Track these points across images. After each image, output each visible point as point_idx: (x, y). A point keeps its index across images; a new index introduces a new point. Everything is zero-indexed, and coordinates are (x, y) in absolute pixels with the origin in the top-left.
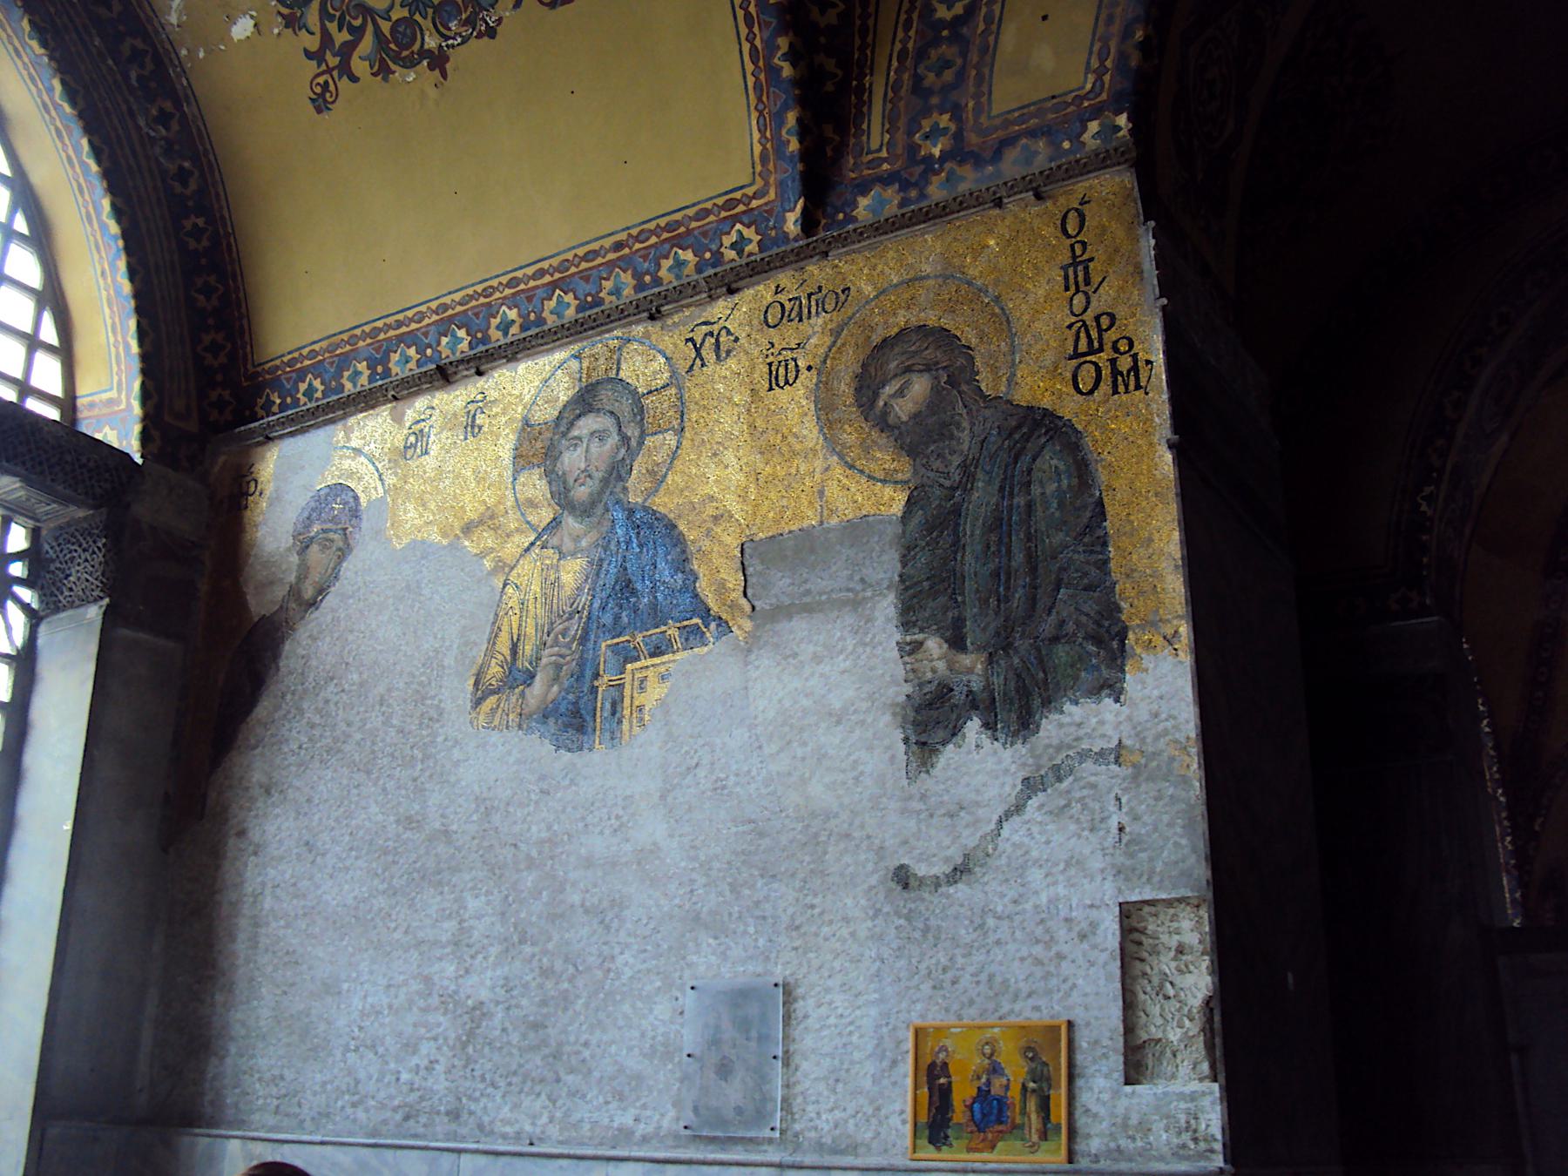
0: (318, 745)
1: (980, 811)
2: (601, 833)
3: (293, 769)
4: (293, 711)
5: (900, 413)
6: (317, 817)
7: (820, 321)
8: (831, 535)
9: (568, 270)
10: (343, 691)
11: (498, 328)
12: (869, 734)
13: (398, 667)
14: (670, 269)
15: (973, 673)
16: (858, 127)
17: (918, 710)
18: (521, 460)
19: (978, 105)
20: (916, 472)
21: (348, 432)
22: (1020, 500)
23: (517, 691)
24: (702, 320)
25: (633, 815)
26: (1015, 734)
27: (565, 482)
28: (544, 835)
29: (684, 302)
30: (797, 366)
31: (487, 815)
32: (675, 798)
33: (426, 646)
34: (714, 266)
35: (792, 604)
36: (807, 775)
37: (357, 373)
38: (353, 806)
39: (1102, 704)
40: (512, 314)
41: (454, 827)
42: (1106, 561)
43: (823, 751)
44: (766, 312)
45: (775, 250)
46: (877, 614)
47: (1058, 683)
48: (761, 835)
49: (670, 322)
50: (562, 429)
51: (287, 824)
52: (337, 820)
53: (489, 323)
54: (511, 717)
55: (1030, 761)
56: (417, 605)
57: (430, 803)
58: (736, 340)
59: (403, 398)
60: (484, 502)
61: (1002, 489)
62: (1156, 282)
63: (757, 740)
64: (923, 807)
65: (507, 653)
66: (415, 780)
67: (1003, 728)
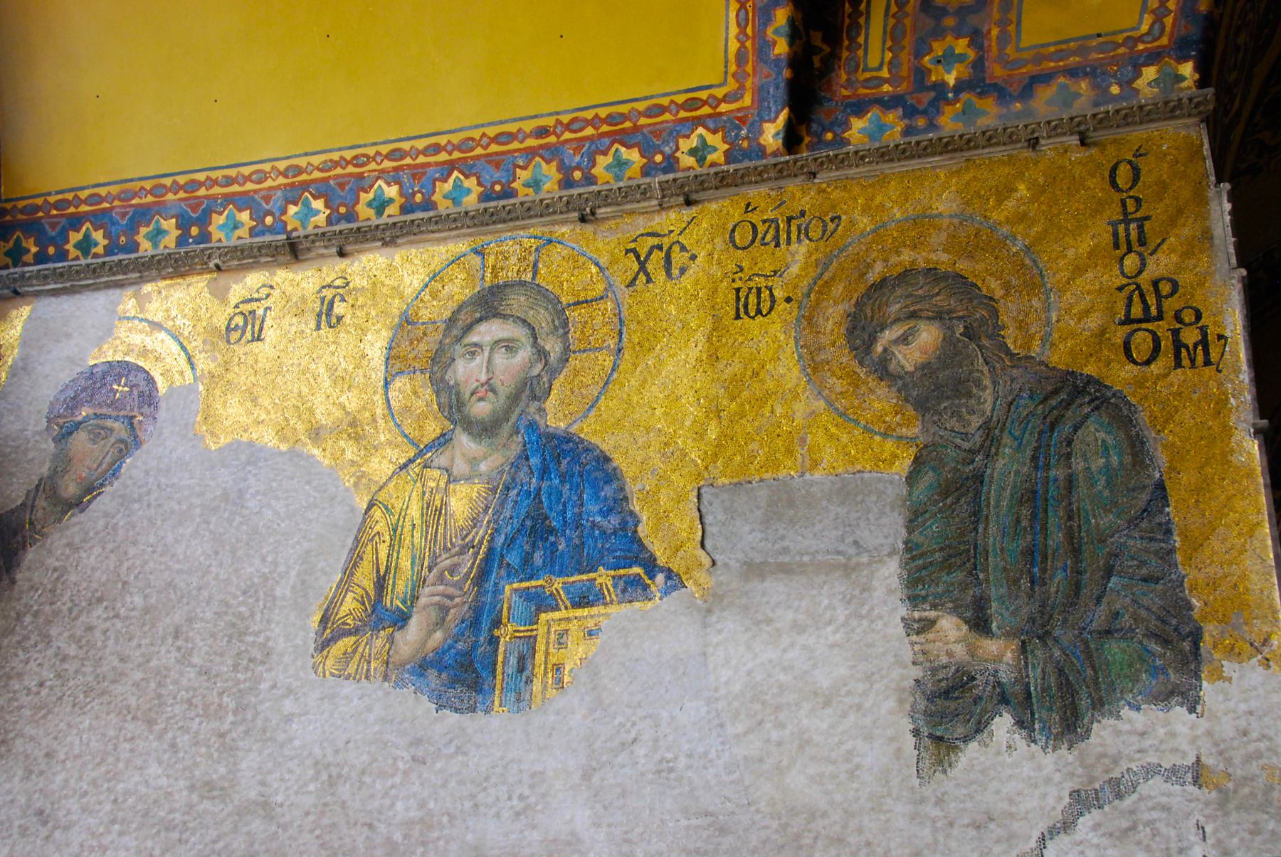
0: (71, 683)
1: (1016, 826)
2: (498, 815)
3: (27, 712)
4: (34, 638)
5: (903, 362)
6: (59, 779)
7: (803, 249)
8: (814, 489)
9: (472, 150)
10: (117, 616)
11: (369, 204)
12: (868, 721)
13: (205, 594)
14: (608, 168)
15: (1001, 662)
16: (852, 40)
17: (931, 698)
18: (395, 362)
19: (1003, 32)
20: (925, 430)
21: (142, 301)
22: (1058, 473)
23: (382, 633)
24: (650, 231)
25: (544, 796)
26: (1058, 737)
27: (458, 394)
28: (414, 814)
29: (628, 207)
30: (772, 295)
31: (331, 785)
32: (603, 780)
33: (250, 570)
34: (665, 171)
35: (764, 563)
36: (785, 763)
37: (159, 232)
38: (121, 765)
39: (1171, 713)
40: (392, 191)
41: (279, 799)
42: (1171, 551)
43: (806, 736)
44: (733, 231)
45: (746, 164)
46: (875, 583)
47: (1112, 683)
48: (723, 831)
49: (604, 227)
50: (455, 332)
52: (94, 783)
53: (358, 197)
54: (373, 665)
55: (1080, 771)
56: (238, 519)
57: (244, 765)
58: (693, 257)
59: (229, 270)
60: (344, 408)
61: (1034, 458)
62: (1232, 250)
63: (718, 716)
64: (940, 814)
65: (369, 585)
66: (222, 735)
67: (1043, 729)
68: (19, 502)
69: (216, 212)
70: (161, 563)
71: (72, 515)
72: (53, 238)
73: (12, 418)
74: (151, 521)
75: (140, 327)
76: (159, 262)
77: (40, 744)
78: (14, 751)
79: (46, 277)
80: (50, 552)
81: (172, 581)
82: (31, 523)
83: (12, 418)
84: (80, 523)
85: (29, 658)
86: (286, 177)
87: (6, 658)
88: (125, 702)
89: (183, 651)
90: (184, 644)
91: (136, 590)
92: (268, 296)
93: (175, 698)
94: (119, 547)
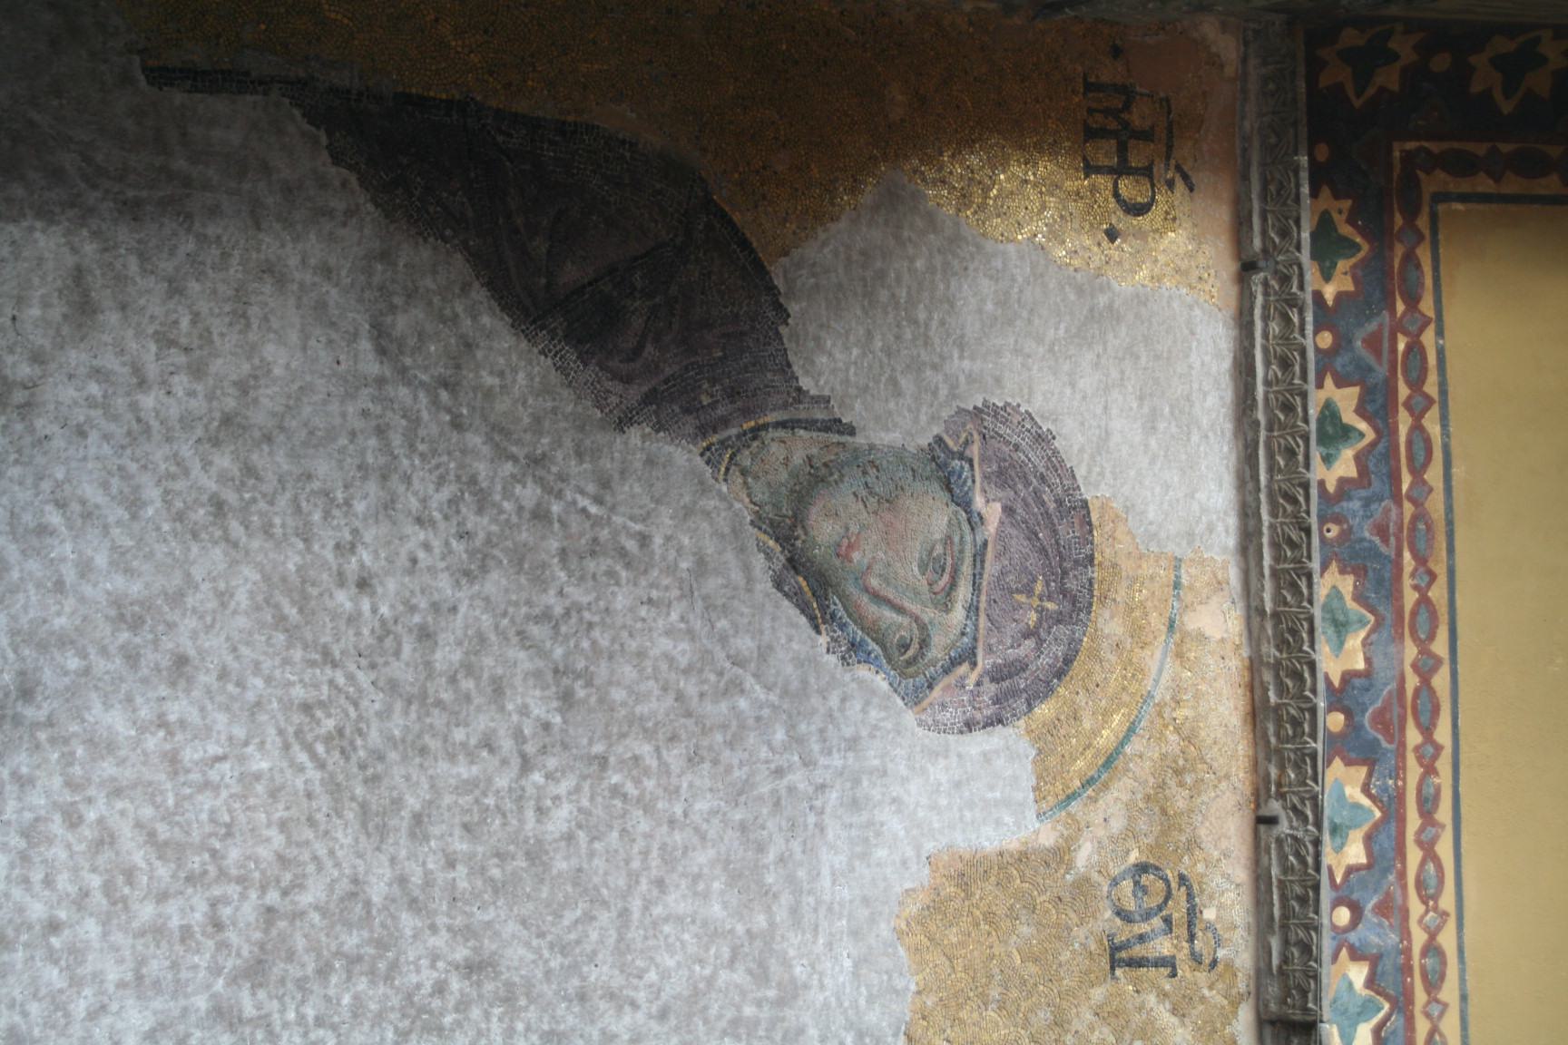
0: (364, 678)
4: (481, 524)
6: (116, 721)
51: (101, 560)
52: (106, 839)
59: (1258, 848)
68: (805, 383)
69: (1370, 775)
70: (645, 853)
71: (769, 557)
72: (1350, 341)
73: (989, 307)
74: (739, 793)
75: (1157, 622)
76: (1297, 676)
77: (209, 628)
78: (195, 549)
79: (1285, 364)
80: (688, 512)
81: (605, 904)
82: (756, 432)
83: (989, 307)
84: (750, 580)
85: (433, 523)
86: (1424, 953)
87: (434, 452)
88: (311, 868)
89: (436, 1003)
90: (451, 1002)
91: (585, 803)
92: (1196, 958)
93: (320, 1022)
94: (689, 714)
